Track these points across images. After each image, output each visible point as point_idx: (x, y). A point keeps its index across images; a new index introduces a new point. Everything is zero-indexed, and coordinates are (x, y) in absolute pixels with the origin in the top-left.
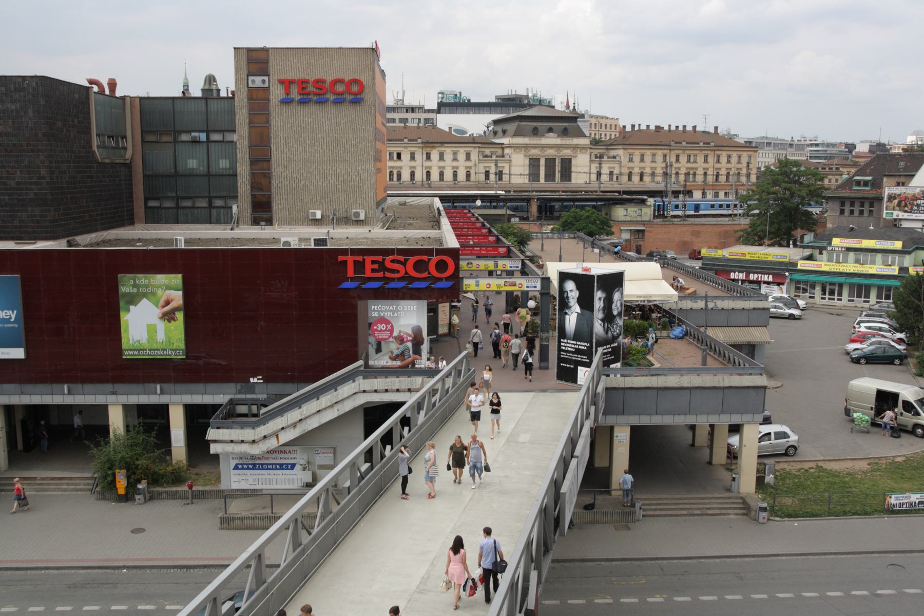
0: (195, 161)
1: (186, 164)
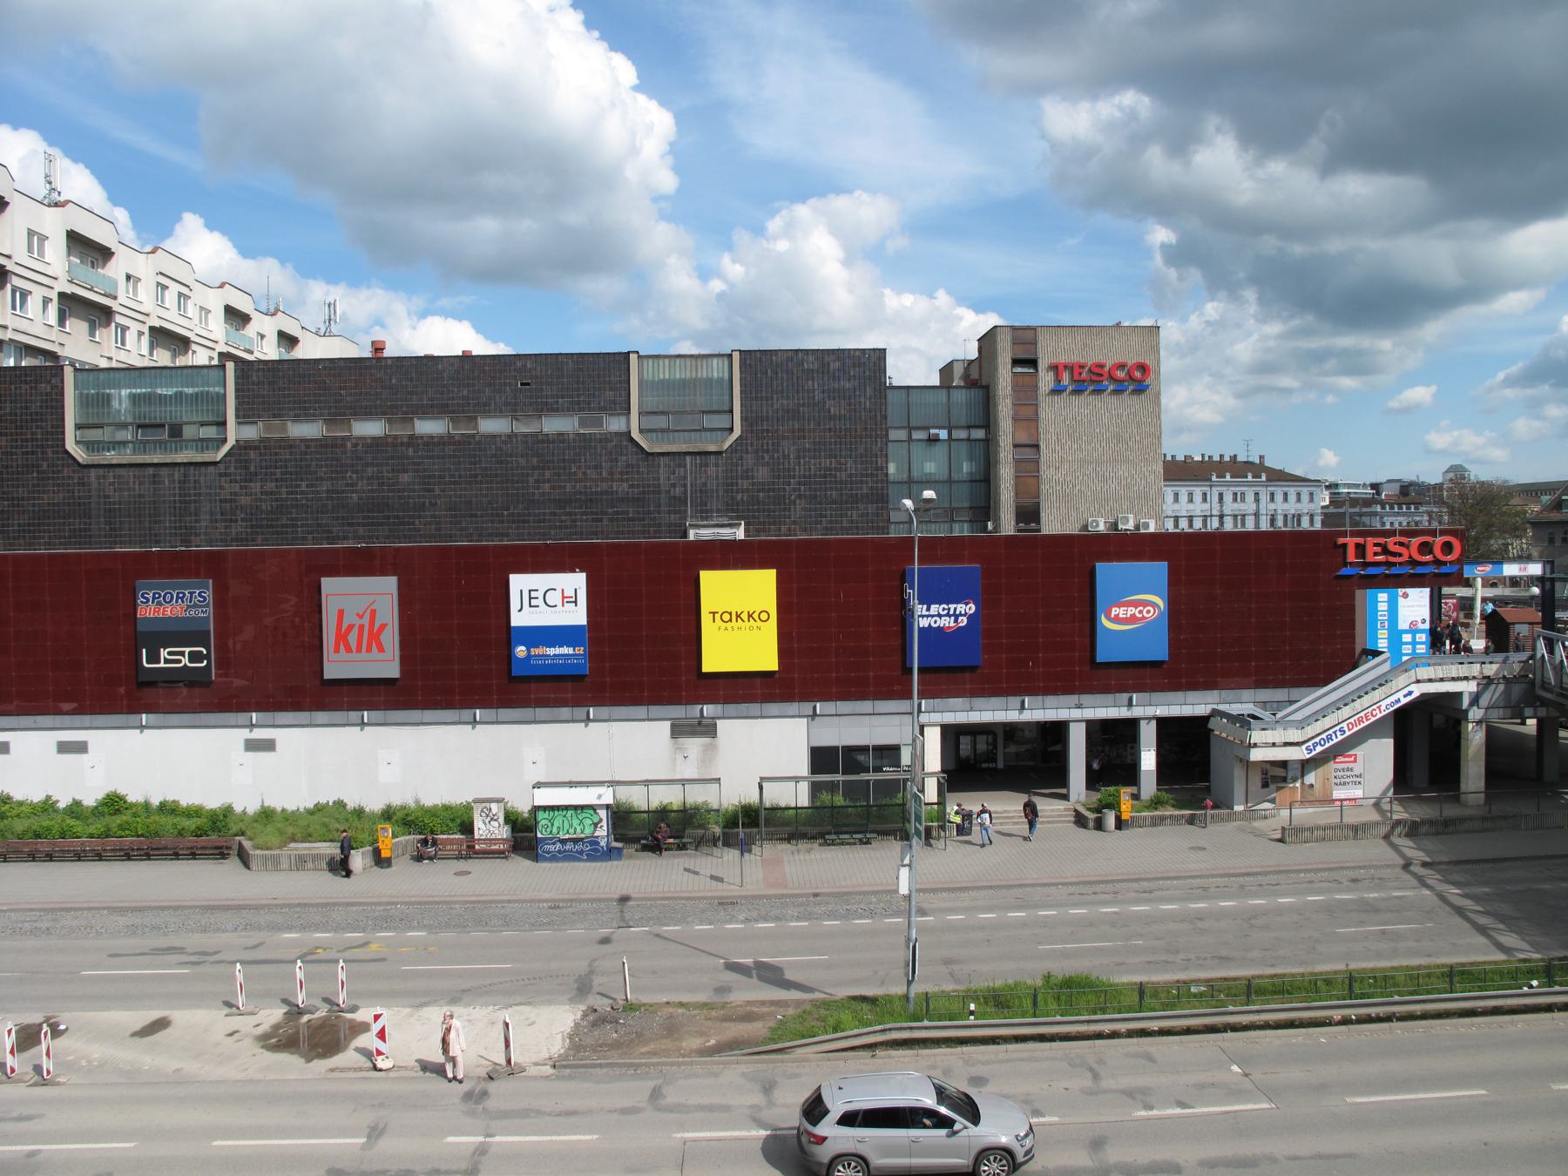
0: (932, 464)
1: (923, 469)
